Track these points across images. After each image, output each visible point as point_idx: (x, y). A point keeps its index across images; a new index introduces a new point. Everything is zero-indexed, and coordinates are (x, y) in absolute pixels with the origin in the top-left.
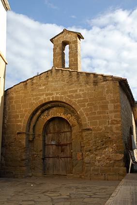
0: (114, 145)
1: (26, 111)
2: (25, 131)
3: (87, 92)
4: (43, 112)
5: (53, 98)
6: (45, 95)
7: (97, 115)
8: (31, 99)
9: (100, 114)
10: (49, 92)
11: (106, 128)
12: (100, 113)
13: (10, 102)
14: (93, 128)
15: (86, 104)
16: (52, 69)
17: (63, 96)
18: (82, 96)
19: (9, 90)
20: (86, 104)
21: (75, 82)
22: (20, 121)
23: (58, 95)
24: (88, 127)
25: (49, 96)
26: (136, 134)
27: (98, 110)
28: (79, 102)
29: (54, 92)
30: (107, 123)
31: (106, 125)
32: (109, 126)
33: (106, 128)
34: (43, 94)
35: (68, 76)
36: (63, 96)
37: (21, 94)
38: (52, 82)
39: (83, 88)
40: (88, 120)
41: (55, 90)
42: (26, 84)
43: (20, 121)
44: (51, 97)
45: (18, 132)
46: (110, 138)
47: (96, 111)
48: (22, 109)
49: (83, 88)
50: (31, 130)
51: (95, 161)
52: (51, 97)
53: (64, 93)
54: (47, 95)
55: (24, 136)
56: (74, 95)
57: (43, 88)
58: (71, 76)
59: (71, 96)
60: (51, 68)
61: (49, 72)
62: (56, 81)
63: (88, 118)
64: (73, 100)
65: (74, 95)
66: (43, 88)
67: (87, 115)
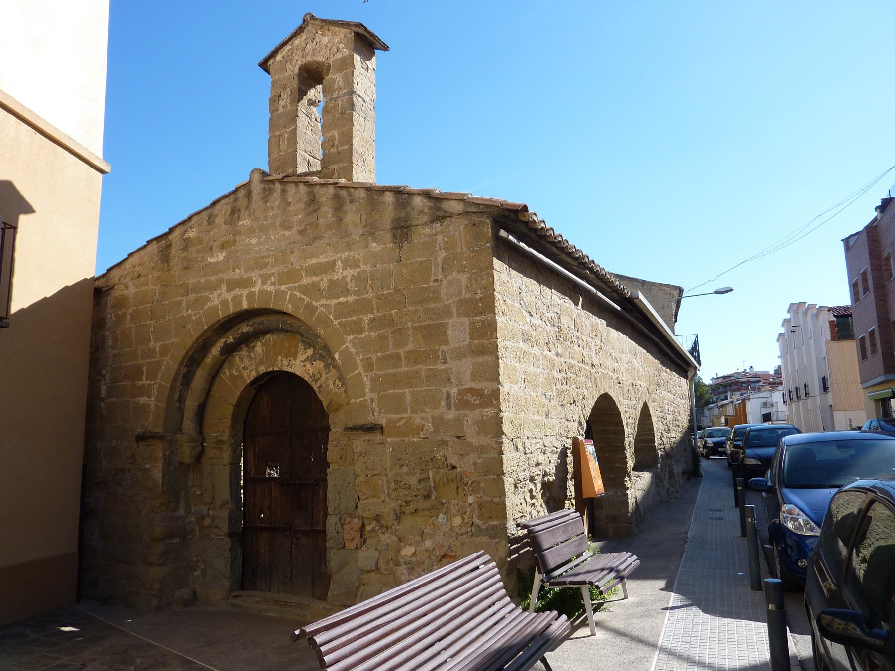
0: (471, 499)
1: (164, 351)
2: (159, 430)
3: (368, 268)
4: (229, 351)
5: (250, 296)
6: (224, 288)
7: (404, 369)
8: (180, 303)
9: (416, 363)
10: (239, 273)
11: (439, 422)
12: (416, 357)
13: (117, 316)
14: (390, 421)
15: (366, 318)
16: (249, 182)
17: (283, 288)
18: (352, 286)
19: (115, 273)
20: (366, 318)
21: (329, 227)
22: (146, 391)
23: (269, 288)
24: (370, 419)
25: (237, 291)
26: (523, 549)
27: (410, 347)
28: (343, 310)
29: (254, 275)
30: (443, 403)
31: (437, 412)
32: (451, 415)
33: (439, 422)
34: (216, 286)
35: (302, 206)
36: (283, 288)
37: (151, 287)
38: (251, 232)
39: (354, 254)
40: (372, 391)
41: (259, 264)
42: (169, 246)
43: (146, 391)
44: (245, 292)
45: (139, 431)
46: (454, 468)
47: (401, 351)
48: (151, 344)
49: (354, 254)
50: (189, 425)
51: (398, 564)
52: (245, 292)
53: (290, 276)
54: (233, 285)
55: (159, 450)
56: (324, 284)
57: (221, 257)
58: (313, 207)
59: (312, 290)
60: (246, 180)
61: (241, 194)
62: (263, 229)
63: (374, 380)
64: (320, 304)
65: (324, 284)
66: (221, 257)
67: (369, 367)
